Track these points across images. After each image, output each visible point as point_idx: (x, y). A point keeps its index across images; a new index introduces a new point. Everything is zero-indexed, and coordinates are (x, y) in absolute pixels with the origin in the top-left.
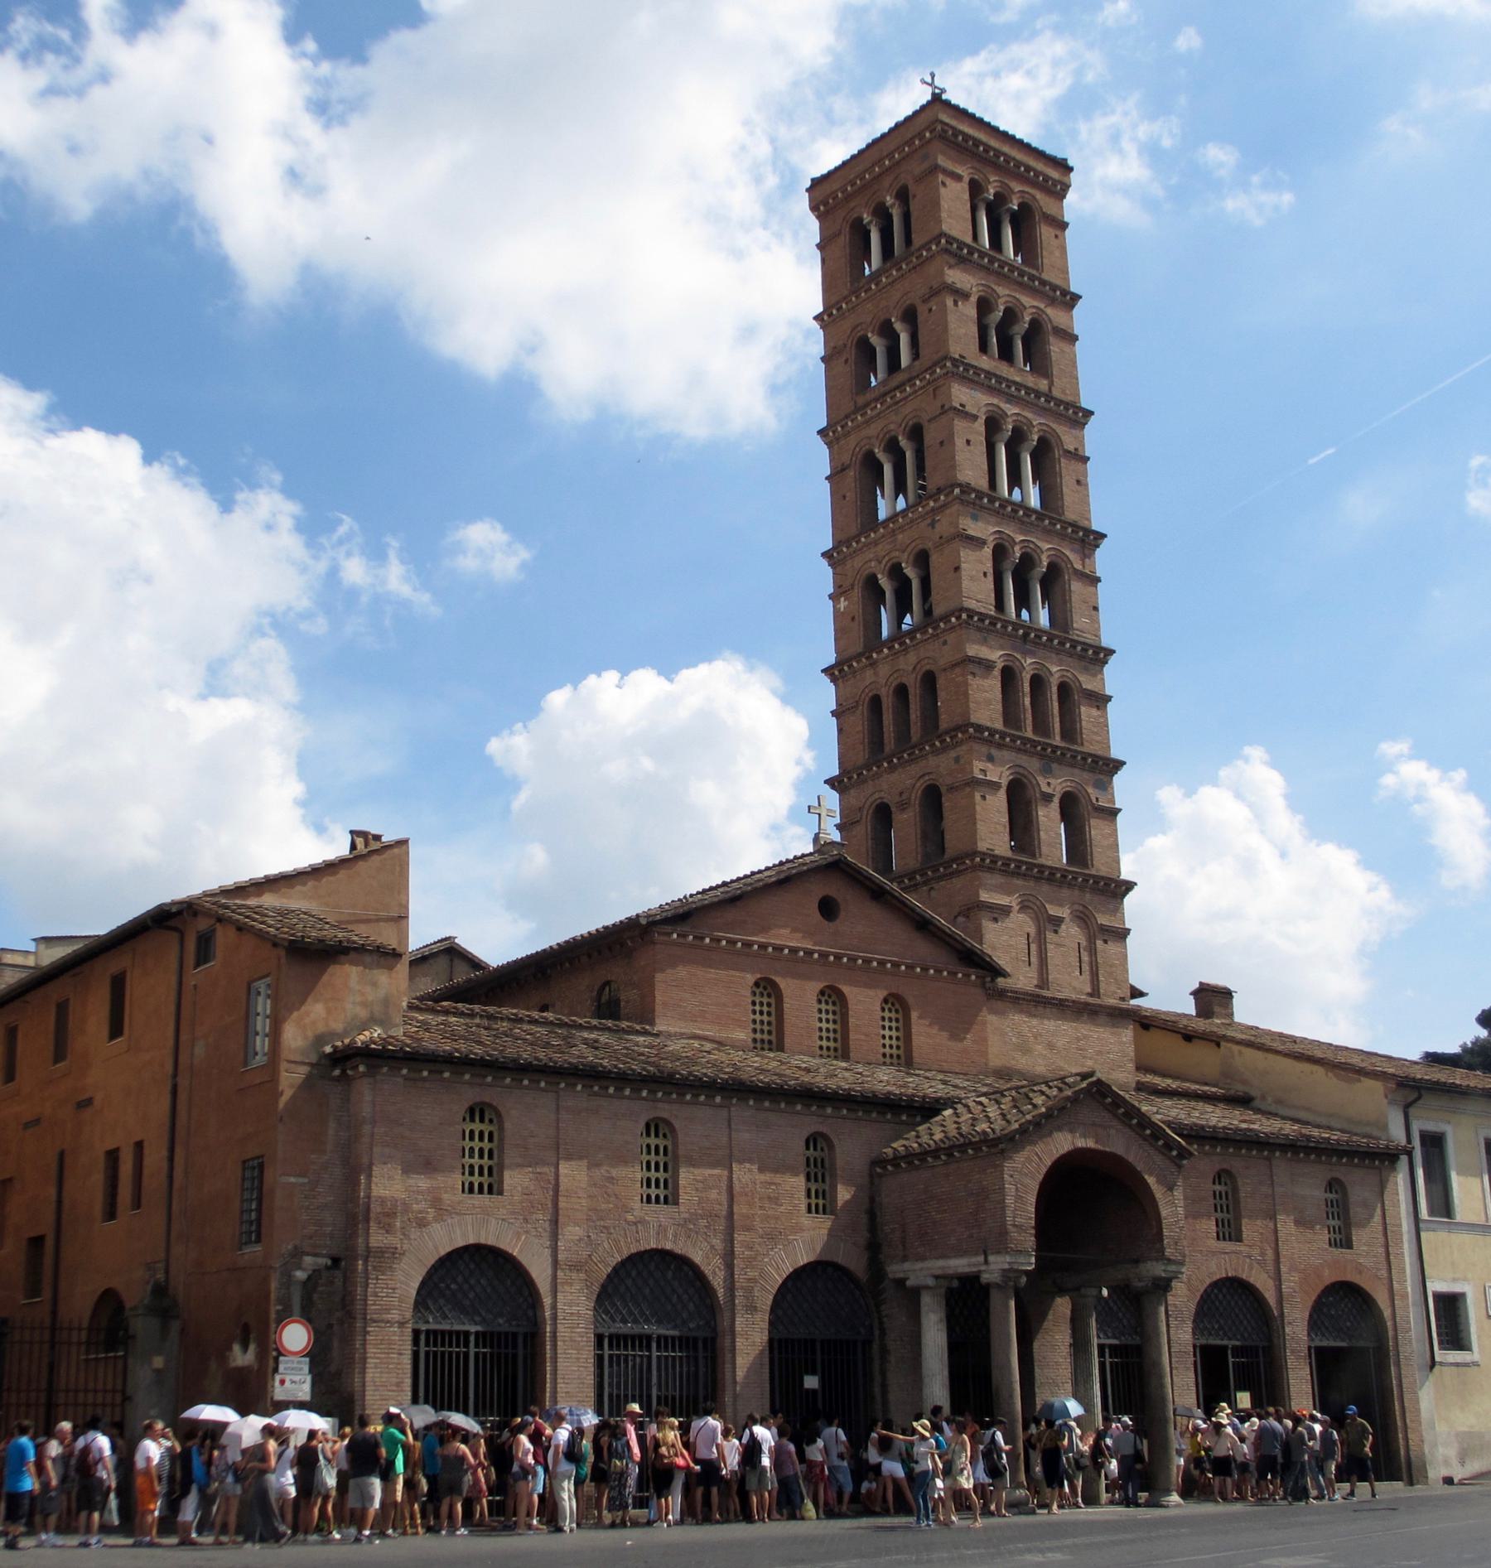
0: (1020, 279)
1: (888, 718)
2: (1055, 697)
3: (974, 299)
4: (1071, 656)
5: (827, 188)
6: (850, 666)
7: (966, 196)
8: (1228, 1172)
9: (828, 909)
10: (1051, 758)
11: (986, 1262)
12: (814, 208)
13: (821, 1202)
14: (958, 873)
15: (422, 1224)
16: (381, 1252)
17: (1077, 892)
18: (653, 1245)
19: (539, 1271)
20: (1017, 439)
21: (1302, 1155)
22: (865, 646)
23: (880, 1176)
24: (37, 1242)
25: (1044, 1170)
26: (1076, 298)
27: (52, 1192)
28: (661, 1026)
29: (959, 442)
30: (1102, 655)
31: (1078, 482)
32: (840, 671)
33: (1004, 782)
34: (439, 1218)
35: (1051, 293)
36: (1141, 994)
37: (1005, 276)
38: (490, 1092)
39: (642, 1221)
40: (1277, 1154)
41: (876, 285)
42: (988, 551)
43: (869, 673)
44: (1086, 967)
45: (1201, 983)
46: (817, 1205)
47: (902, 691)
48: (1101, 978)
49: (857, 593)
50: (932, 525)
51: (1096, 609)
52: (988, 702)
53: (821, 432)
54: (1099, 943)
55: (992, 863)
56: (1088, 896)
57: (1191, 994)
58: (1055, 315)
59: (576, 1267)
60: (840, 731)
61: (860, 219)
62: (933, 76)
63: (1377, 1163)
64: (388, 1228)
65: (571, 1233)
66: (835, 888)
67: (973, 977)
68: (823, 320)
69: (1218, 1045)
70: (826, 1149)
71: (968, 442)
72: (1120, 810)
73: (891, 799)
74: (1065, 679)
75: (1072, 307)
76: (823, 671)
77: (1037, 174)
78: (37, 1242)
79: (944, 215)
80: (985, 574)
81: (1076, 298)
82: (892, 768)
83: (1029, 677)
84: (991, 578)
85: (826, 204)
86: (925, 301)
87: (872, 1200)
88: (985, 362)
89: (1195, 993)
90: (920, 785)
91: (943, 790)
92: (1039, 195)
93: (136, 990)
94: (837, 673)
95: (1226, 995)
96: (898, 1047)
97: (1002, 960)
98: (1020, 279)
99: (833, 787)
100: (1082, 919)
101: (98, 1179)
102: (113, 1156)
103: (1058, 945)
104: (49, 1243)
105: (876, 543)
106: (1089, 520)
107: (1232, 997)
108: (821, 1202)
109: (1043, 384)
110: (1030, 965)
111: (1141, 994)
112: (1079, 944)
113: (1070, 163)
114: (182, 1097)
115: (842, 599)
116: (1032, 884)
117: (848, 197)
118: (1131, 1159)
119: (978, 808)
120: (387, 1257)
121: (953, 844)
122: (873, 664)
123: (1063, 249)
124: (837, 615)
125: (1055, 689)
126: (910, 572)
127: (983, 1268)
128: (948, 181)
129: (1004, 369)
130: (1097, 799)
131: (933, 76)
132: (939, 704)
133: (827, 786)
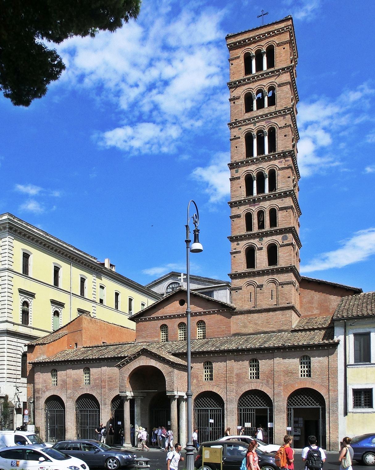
4: (275, 199)
10: (260, 236)
44: (274, 297)
71: (236, 147)
74: (272, 207)
77: (273, 32)
83: (256, 213)
109: (272, 109)
112: (272, 290)
130: (283, 242)
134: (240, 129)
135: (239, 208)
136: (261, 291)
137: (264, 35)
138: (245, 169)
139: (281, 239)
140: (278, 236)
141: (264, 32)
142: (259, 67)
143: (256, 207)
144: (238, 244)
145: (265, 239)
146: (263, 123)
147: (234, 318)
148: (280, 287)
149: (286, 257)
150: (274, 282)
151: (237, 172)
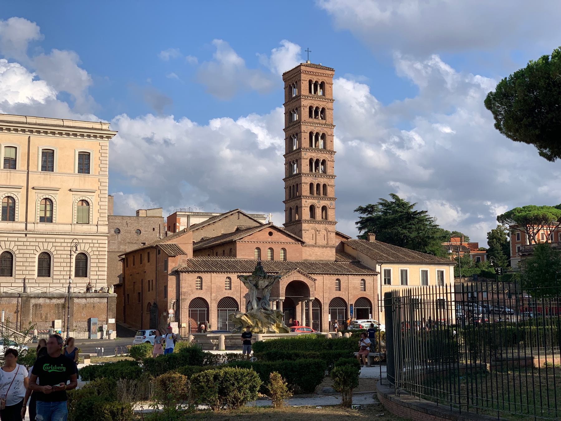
1: (292, 191)
2: (322, 187)
3: (308, 107)
5: (286, 76)
9: (271, 234)
12: (283, 80)
15: (190, 295)
16: (184, 299)
17: (324, 225)
18: (227, 296)
19: (208, 301)
20: (317, 134)
22: (289, 176)
24: (139, 293)
27: (141, 285)
28: (237, 257)
29: (303, 139)
31: (331, 141)
33: (309, 206)
34: (192, 294)
35: (327, 101)
38: (200, 275)
39: (225, 292)
42: (308, 160)
43: (289, 181)
44: (326, 239)
49: (288, 164)
50: (298, 155)
52: (306, 191)
56: (327, 225)
58: (329, 105)
59: (214, 300)
64: (185, 296)
65: (213, 295)
73: (292, 207)
78: (139, 293)
79: (302, 90)
84: (308, 165)
86: (299, 108)
88: (311, 120)
90: (295, 206)
92: (326, 78)
93: (151, 255)
101: (147, 284)
102: (149, 281)
103: (319, 236)
104: (141, 293)
105: (291, 156)
106: (333, 149)
109: (324, 121)
111: (351, 238)
114: (157, 274)
116: (314, 224)
117: (289, 80)
118: (304, 281)
119: (303, 212)
120: (184, 300)
123: (332, 90)
125: (322, 186)
128: (303, 82)
134: (307, 127)
135: (306, 178)
136: (319, 234)
137: (321, 74)
138: (309, 154)
140: (328, 202)
141: (321, 72)
144: (306, 202)
145: (321, 201)
146: (320, 129)
147: (305, 249)
148: (329, 233)
149: (333, 215)
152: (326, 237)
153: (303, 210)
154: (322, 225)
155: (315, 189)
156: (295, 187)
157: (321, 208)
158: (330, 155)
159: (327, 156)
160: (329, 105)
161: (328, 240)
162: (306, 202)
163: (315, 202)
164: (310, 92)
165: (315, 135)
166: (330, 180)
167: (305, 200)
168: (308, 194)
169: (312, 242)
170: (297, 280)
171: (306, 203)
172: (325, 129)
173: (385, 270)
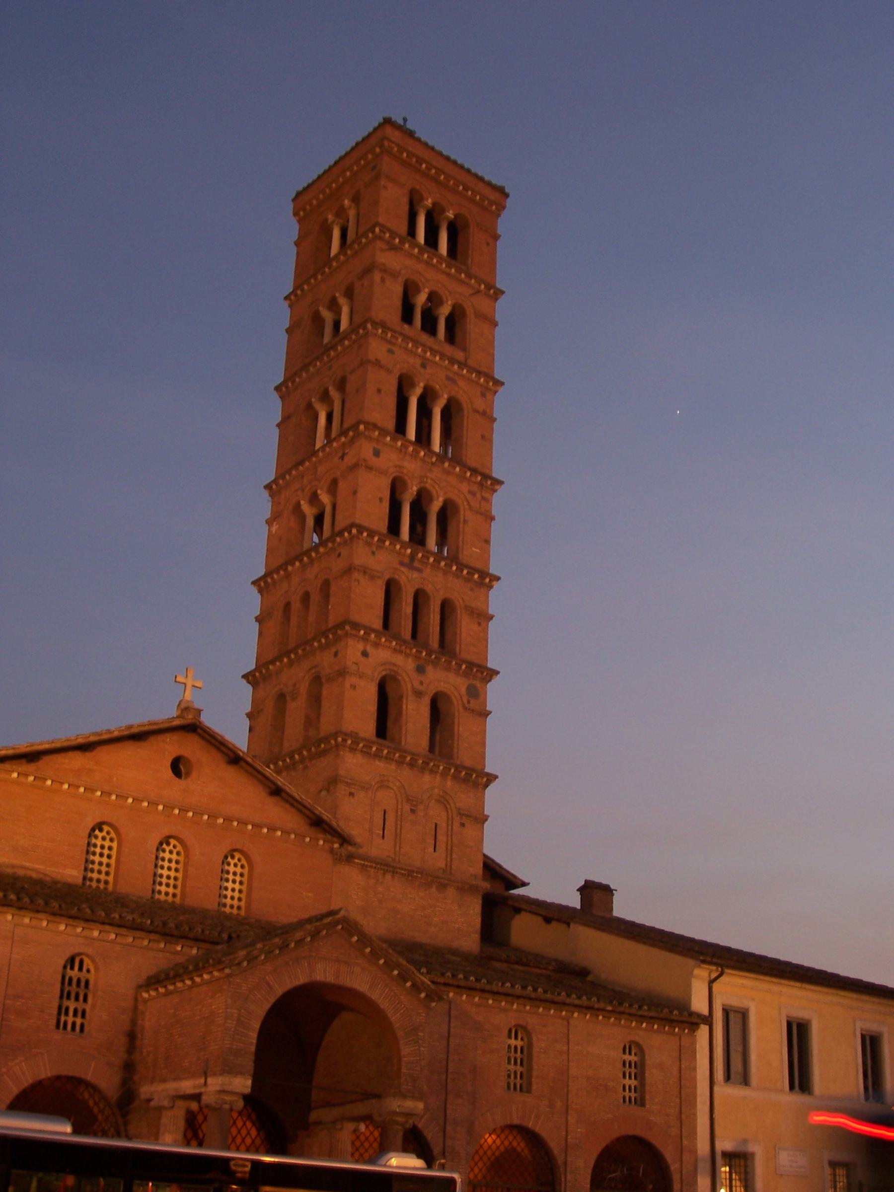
0: (447, 270)
3: (401, 280)
6: (272, 578)
7: (405, 200)
8: (524, 1028)
11: (206, 1083)
12: (295, 214)
13: (79, 1021)
14: (324, 753)
21: (601, 1018)
23: (146, 1001)
25: (272, 1000)
26: (499, 293)
30: (487, 580)
31: (483, 437)
32: (266, 582)
36: (524, 884)
37: (433, 265)
40: (576, 1015)
41: (329, 268)
42: (385, 484)
45: (586, 881)
46: (74, 1024)
47: (306, 598)
48: (454, 856)
50: (342, 458)
51: (487, 542)
53: (278, 389)
54: (456, 825)
55: (355, 741)
57: (578, 890)
60: (261, 634)
61: (326, 220)
62: (405, 120)
63: (677, 1030)
66: (190, 748)
67: (321, 842)
68: (290, 300)
69: (568, 925)
70: (92, 970)
71: (379, 391)
72: (490, 713)
75: (496, 299)
76: (254, 583)
80: (381, 500)
81: (499, 293)
82: (291, 664)
85: (304, 210)
87: (134, 1022)
89: (581, 890)
91: (324, 680)
94: (262, 584)
95: (607, 891)
96: (240, 899)
97: (355, 832)
98: (447, 270)
99: (249, 682)
100: (443, 803)
107: (613, 895)
108: (79, 1021)
109: (460, 355)
110: (383, 837)
111: (524, 884)
113: (507, 190)
115: (275, 523)
118: (374, 996)
121: (326, 726)
122: (288, 576)
124: (270, 536)
126: (325, 498)
127: (203, 1090)
129: (425, 338)
130: (469, 702)
131: (405, 120)
132: (330, 607)
133: (244, 681)
139: (463, 690)
142: (432, 240)
143: (416, 575)
145: (430, 669)
150: (444, 801)
151: (377, 453)
152: (441, 838)
153: (347, 685)
154: (427, 778)
155: (408, 610)
156: (315, 598)
157: (426, 701)
158: (475, 488)
159: (464, 487)
160: (482, 303)
161: (450, 851)
162: (365, 654)
163: (405, 664)
164: (412, 232)
165: (418, 391)
166: (471, 589)
167: (360, 646)
168: (378, 624)
169: (380, 848)
170: (330, 979)
171: (363, 659)
172: (462, 384)
173: (726, 1012)
